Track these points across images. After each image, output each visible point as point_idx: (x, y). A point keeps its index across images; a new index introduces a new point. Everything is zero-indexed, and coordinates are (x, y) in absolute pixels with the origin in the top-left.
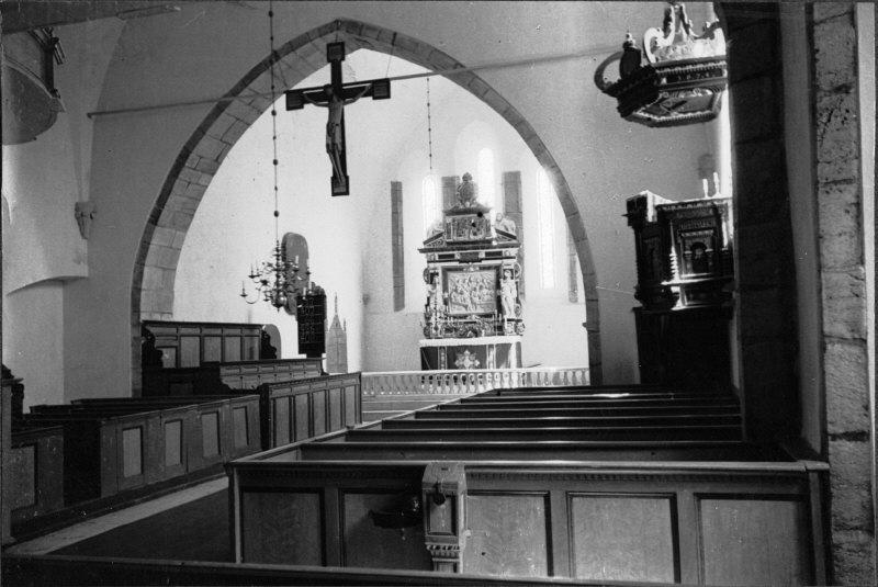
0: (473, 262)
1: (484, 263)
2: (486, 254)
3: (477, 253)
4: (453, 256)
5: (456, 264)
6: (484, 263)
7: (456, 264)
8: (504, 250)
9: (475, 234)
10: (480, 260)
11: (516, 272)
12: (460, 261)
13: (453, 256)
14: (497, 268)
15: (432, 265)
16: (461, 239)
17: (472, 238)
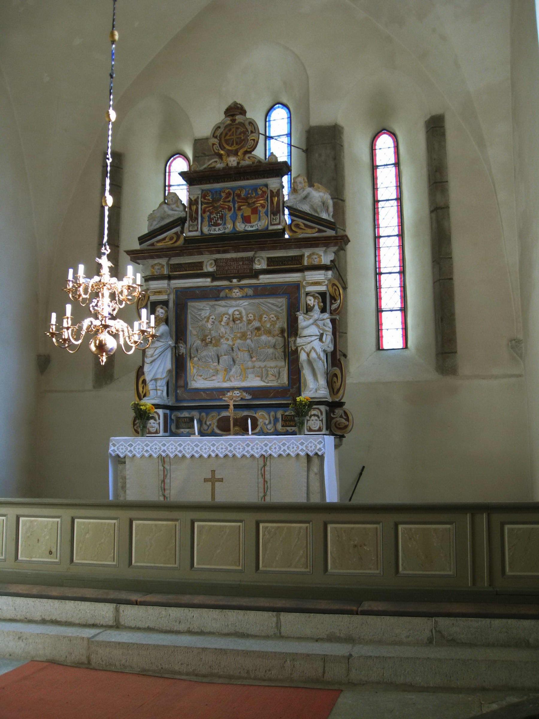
0: (240, 278)
1: (264, 279)
2: (270, 261)
3: (251, 260)
4: (200, 265)
5: (206, 282)
6: (264, 279)
7: (206, 282)
8: (307, 252)
9: (246, 220)
10: (256, 274)
11: (333, 298)
12: (213, 276)
13: (200, 265)
14: (297, 287)
15: (155, 285)
16: (217, 231)
17: (241, 227)
